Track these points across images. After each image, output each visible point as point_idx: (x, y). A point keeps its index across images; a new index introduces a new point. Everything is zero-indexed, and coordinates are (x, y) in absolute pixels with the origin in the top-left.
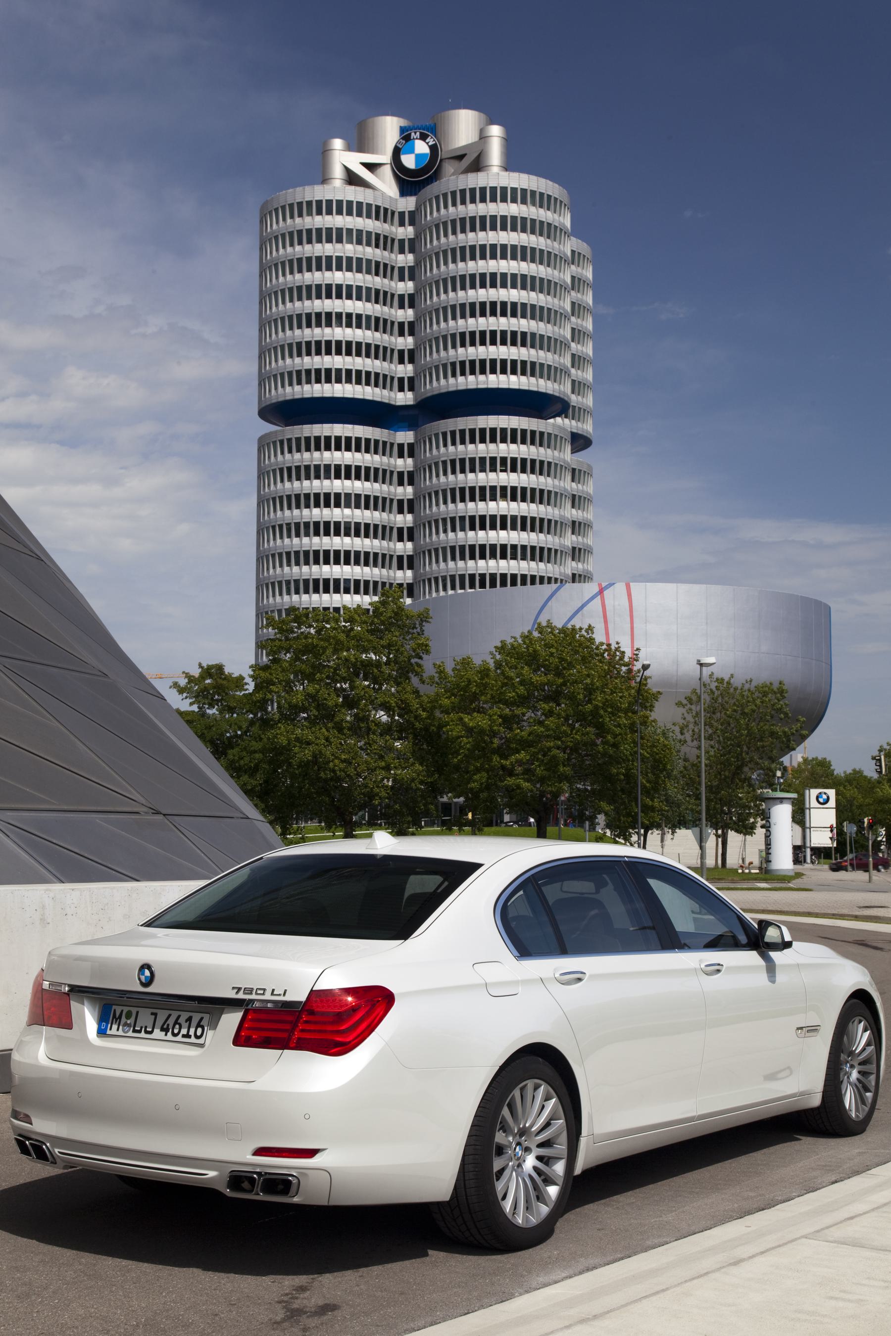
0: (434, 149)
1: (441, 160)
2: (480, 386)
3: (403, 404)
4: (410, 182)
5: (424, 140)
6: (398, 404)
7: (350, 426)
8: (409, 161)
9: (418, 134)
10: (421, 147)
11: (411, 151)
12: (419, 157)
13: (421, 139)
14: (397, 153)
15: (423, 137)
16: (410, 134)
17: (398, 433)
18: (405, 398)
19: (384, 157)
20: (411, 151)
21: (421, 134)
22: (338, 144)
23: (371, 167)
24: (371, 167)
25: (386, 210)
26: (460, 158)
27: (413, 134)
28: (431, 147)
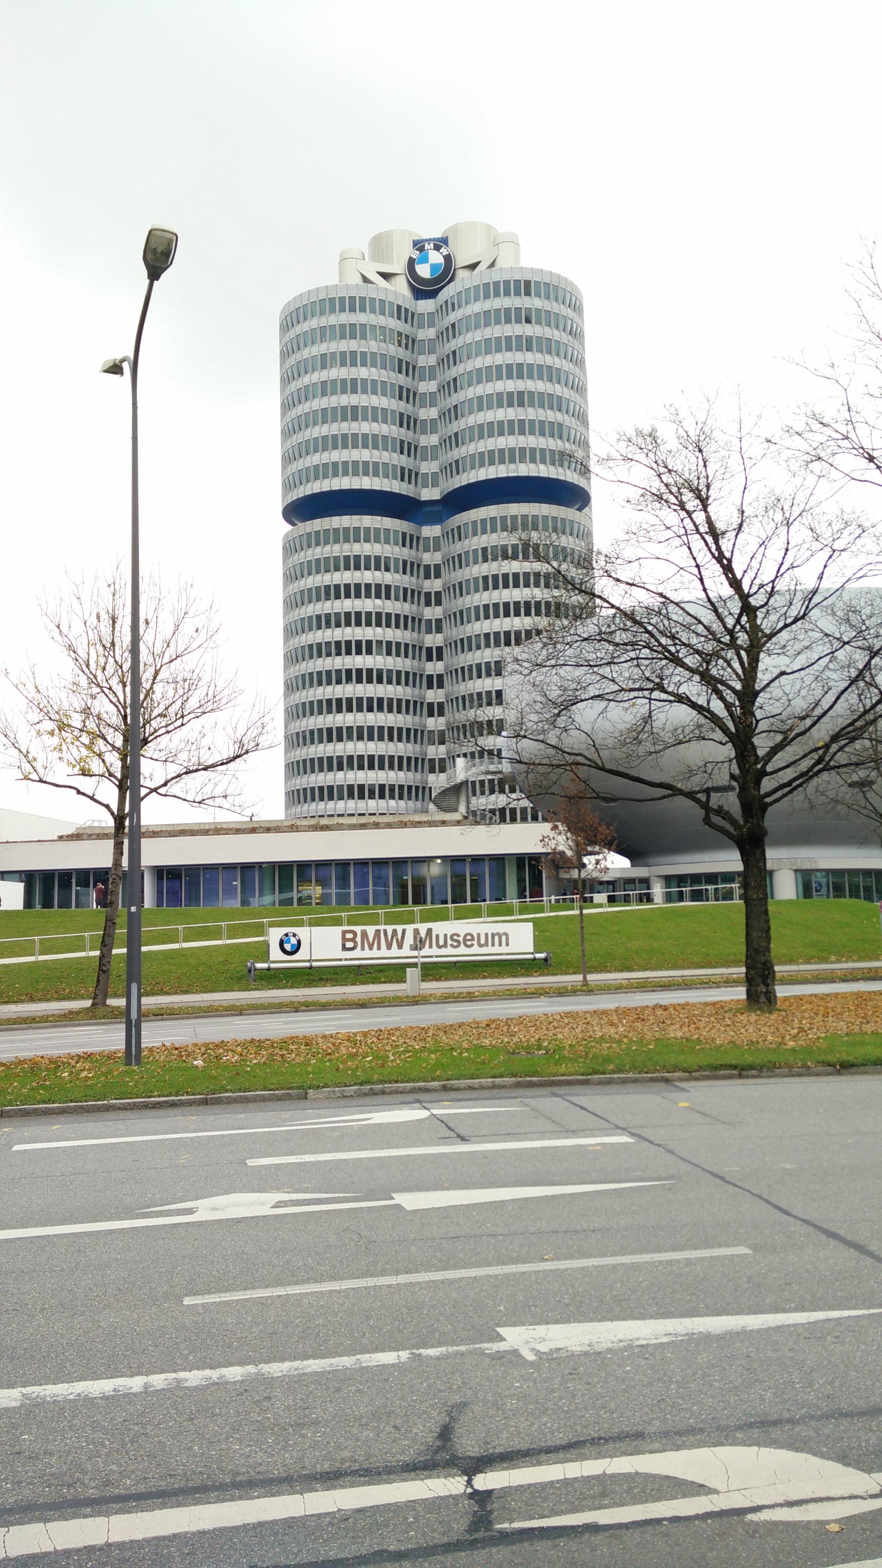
0: (448, 259)
1: (455, 270)
2: (511, 475)
3: (428, 499)
4: (424, 289)
5: (438, 251)
6: (422, 499)
7: (379, 518)
9: (432, 245)
10: (436, 258)
11: (425, 260)
12: (434, 267)
13: (434, 249)
14: (411, 263)
15: (437, 248)
17: (423, 528)
18: (429, 494)
19: (398, 266)
20: (425, 260)
21: (434, 244)
23: (386, 276)
24: (386, 276)
25: (406, 310)
26: (473, 267)
27: (427, 245)
28: (444, 257)
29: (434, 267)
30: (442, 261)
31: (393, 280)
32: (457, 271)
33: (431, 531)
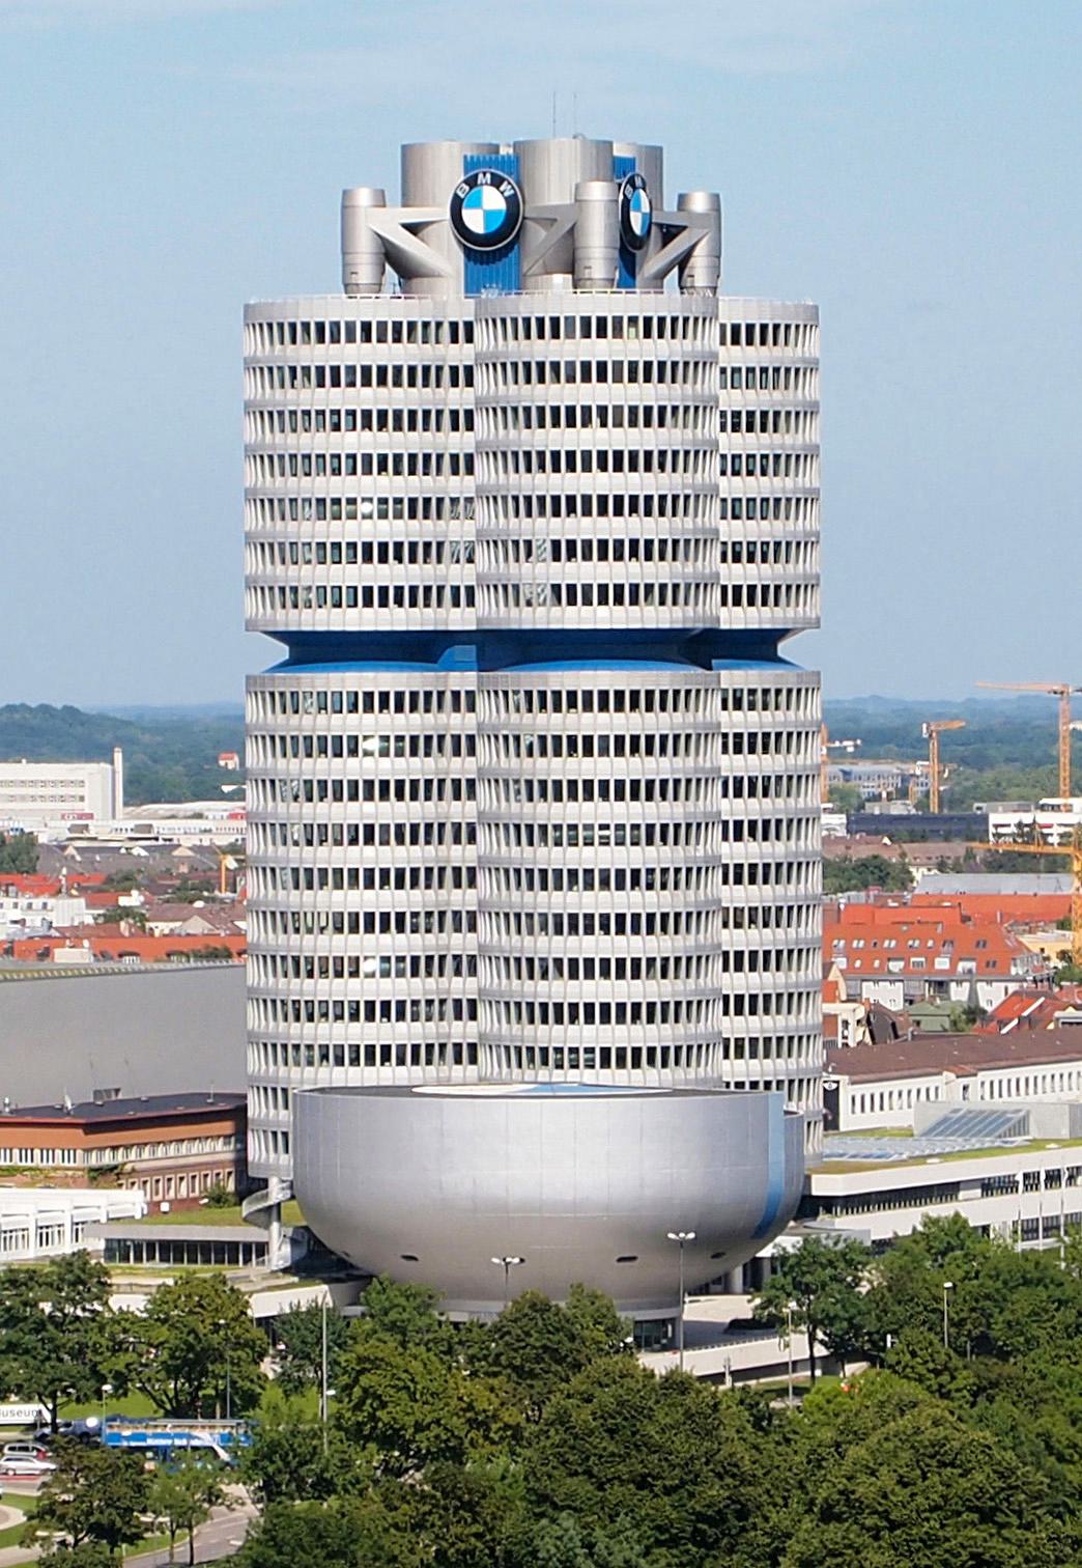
0: (512, 202)
8: (475, 221)
9: (488, 176)
10: (493, 200)
11: (477, 204)
12: (488, 215)
13: (492, 184)
15: (497, 182)
16: (476, 176)
18: (460, 619)
20: (477, 204)
22: (363, 197)
23: (413, 229)
24: (413, 229)
27: (481, 176)
28: (506, 199)
29: (488, 215)
30: (502, 205)
31: (425, 232)
32: (528, 222)
33: (464, 680)
